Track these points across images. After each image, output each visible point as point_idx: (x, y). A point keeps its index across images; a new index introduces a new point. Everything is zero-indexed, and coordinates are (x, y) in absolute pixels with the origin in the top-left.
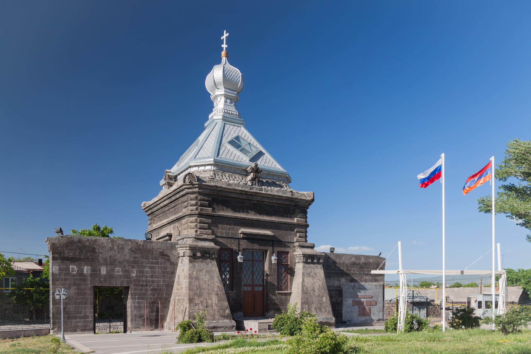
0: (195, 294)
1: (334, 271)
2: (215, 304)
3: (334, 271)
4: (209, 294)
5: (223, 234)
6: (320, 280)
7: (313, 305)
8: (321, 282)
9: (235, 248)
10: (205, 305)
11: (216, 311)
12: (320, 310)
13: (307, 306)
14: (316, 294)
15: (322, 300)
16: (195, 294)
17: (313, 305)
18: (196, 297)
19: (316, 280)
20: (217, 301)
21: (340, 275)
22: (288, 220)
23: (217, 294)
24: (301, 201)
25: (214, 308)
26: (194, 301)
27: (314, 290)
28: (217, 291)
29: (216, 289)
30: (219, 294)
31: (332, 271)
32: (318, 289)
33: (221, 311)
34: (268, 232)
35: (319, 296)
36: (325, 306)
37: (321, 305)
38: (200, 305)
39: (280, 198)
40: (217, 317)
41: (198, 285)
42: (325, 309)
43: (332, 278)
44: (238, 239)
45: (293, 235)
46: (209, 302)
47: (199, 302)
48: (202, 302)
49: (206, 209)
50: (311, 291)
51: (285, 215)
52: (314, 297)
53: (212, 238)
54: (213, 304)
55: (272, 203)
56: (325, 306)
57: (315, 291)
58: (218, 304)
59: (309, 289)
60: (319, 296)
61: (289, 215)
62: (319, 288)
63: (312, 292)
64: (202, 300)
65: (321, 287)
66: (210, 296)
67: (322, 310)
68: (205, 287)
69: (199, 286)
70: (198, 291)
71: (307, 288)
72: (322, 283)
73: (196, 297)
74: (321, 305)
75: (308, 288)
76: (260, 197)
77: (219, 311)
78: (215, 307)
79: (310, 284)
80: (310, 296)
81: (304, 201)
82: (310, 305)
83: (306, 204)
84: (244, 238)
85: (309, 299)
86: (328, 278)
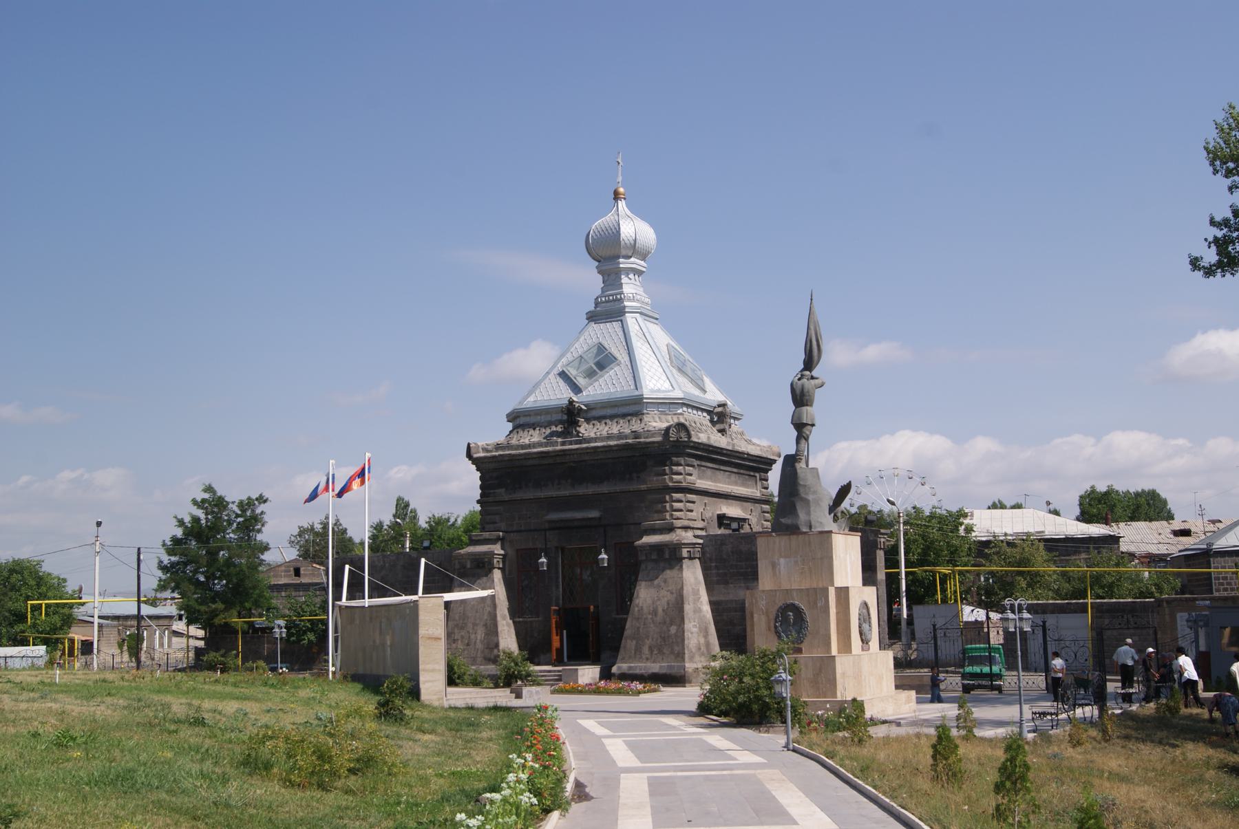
0: (457, 626)
1: (735, 570)
2: (481, 640)
3: (735, 570)
4: (475, 625)
5: (521, 526)
6: (672, 593)
7: (646, 640)
8: (675, 595)
9: (540, 546)
10: (467, 642)
11: (479, 651)
12: (660, 652)
13: (634, 642)
14: (659, 619)
15: (669, 631)
16: (457, 626)
17: (646, 640)
18: (456, 631)
19: (663, 593)
20: (483, 635)
21: (750, 577)
22: (634, 487)
23: (485, 625)
24: (648, 445)
25: (477, 647)
26: (453, 635)
27: (655, 612)
28: (487, 620)
29: (486, 617)
30: (488, 624)
31: (731, 571)
32: (663, 610)
33: (487, 651)
34: (594, 514)
35: (665, 623)
36: (673, 642)
37: (665, 641)
38: (460, 641)
39: (607, 449)
40: (479, 660)
41: (462, 611)
42: (670, 650)
43: (731, 585)
44: (545, 530)
45: (644, 509)
46: (473, 636)
47: (459, 638)
48: (462, 637)
49: (494, 493)
50: (649, 614)
51: (628, 476)
52: (652, 625)
53: (495, 537)
54: (478, 641)
55: (597, 460)
56: (673, 642)
57: (656, 615)
58: (484, 641)
59: (645, 610)
60: (665, 623)
61: (635, 475)
62: (667, 609)
63: (650, 616)
64: (463, 634)
65: (671, 606)
66: (475, 628)
67: (665, 651)
68: (470, 615)
69: (464, 614)
70: (461, 622)
71: (642, 609)
72: (676, 599)
73: (456, 631)
74: (665, 641)
75: (645, 608)
76: (575, 456)
77: (483, 652)
78: (479, 646)
79: (649, 601)
80: (644, 624)
81: (656, 445)
82: (640, 642)
83: (664, 447)
84: (550, 529)
85: (641, 630)
86: (722, 586)
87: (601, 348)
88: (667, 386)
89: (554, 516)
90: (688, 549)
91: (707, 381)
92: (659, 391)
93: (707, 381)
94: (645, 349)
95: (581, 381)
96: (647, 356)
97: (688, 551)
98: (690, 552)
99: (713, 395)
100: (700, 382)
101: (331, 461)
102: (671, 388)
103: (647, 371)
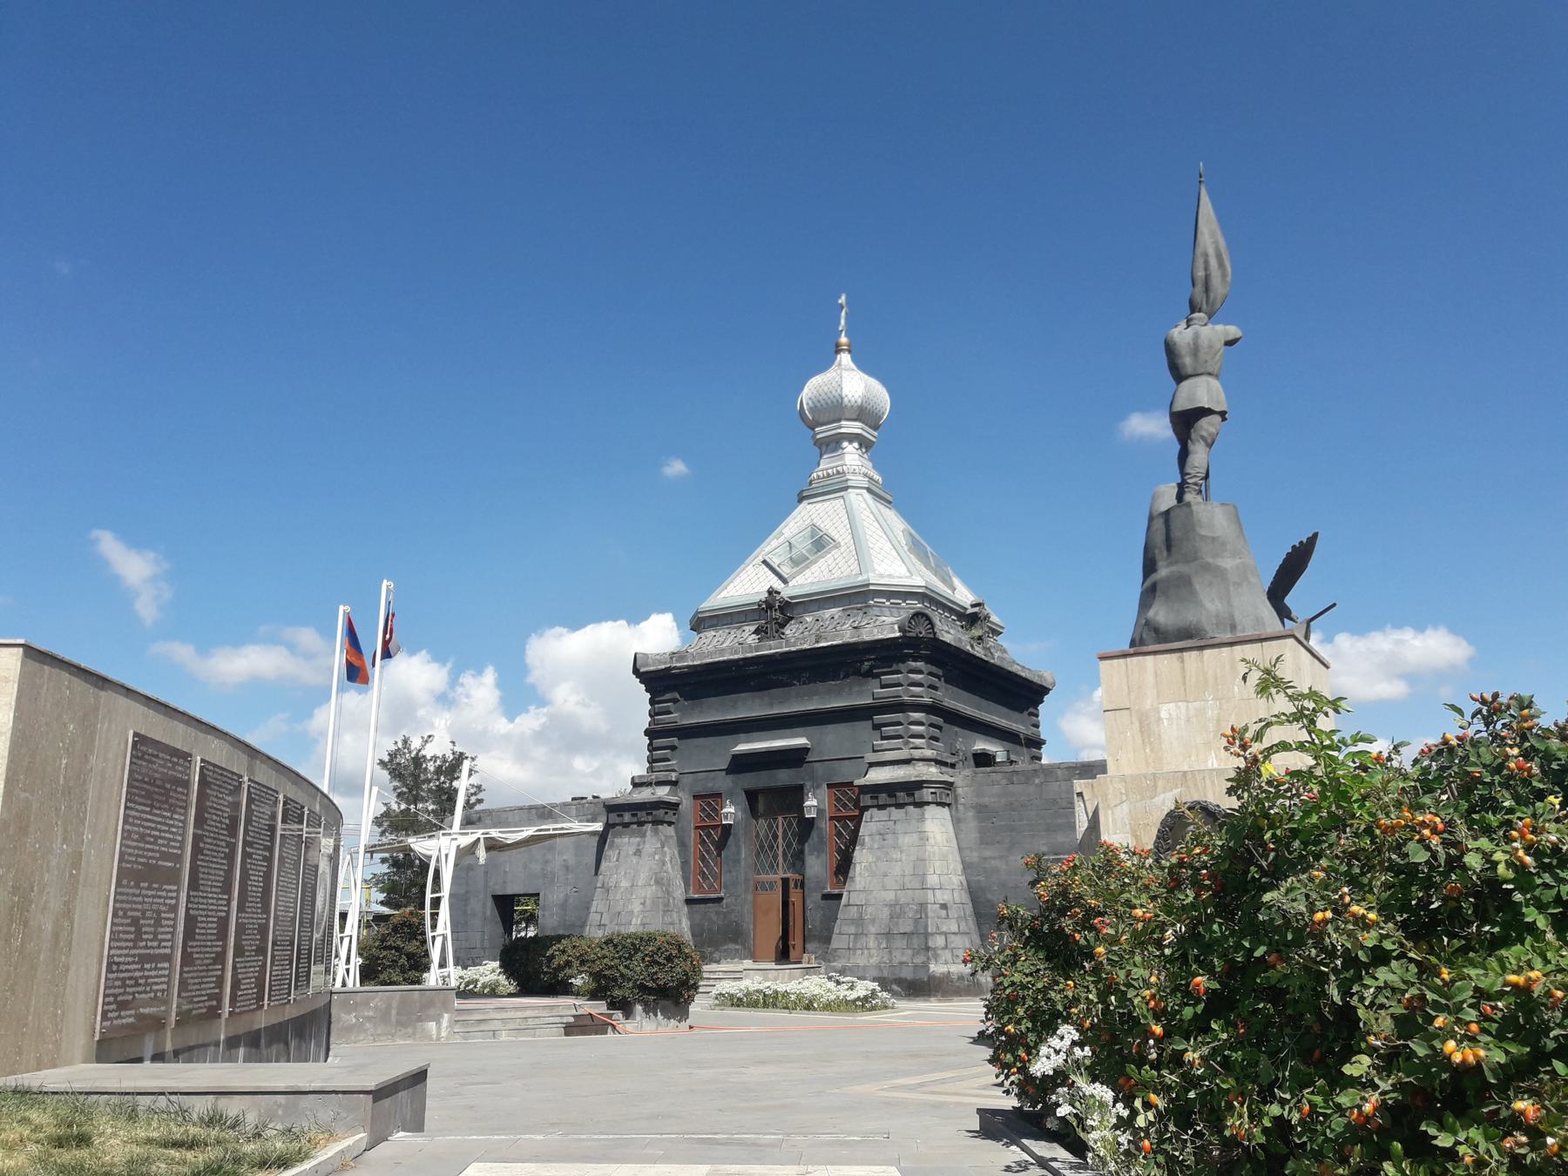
61: (856, 689)
87: (814, 529)
88: (903, 570)
89: (743, 747)
90: (933, 790)
91: (956, 582)
92: (890, 576)
93: (956, 582)
94: (874, 530)
95: (785, 571)
96: (875, 535)
97: (932, 793)
98: (935, 793)
99: (964, 596)
100: (947, 578)
101: (341, 608)
102: (908, 574)
103: (874, 541)
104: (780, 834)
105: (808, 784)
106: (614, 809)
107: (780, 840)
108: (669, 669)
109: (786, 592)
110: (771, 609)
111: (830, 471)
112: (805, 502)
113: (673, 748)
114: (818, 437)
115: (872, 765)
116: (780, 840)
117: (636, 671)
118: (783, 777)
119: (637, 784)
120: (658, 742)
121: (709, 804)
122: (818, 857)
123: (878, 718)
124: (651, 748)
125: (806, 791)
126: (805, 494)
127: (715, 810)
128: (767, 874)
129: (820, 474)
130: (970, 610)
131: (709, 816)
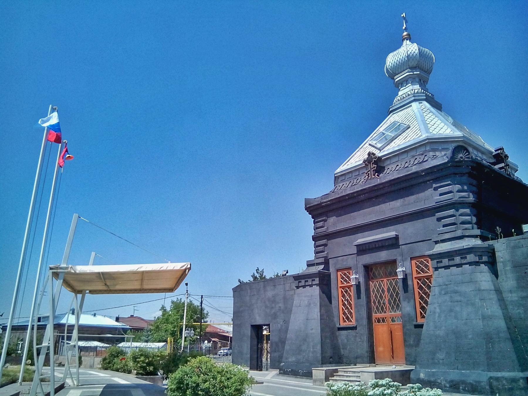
89: (361, 241)
104: (386, 290)
105: (399, 258)
106: (297, 278)
107: (386, 293)
108: (321, 203)
109: (379, 154)
110: (370, 164)
111: (404, 95)
112: (391, 114)
113: (325, 245)
114: (396, 80)
115: (437, 242)
116: (386, 293)
117: (306, 209)
118: (383, 256)
119: (310, 264)
120: (319, 243)
121: (345, 274)
122: (408, 302)
123: (439, 215)
124: (316, 246)
125: (398, 263)
126: (391, 110)
127: (348, 277)
128: (381, 313)
129: (399, 98)
130: (495, 153)
131: (346, 281)
